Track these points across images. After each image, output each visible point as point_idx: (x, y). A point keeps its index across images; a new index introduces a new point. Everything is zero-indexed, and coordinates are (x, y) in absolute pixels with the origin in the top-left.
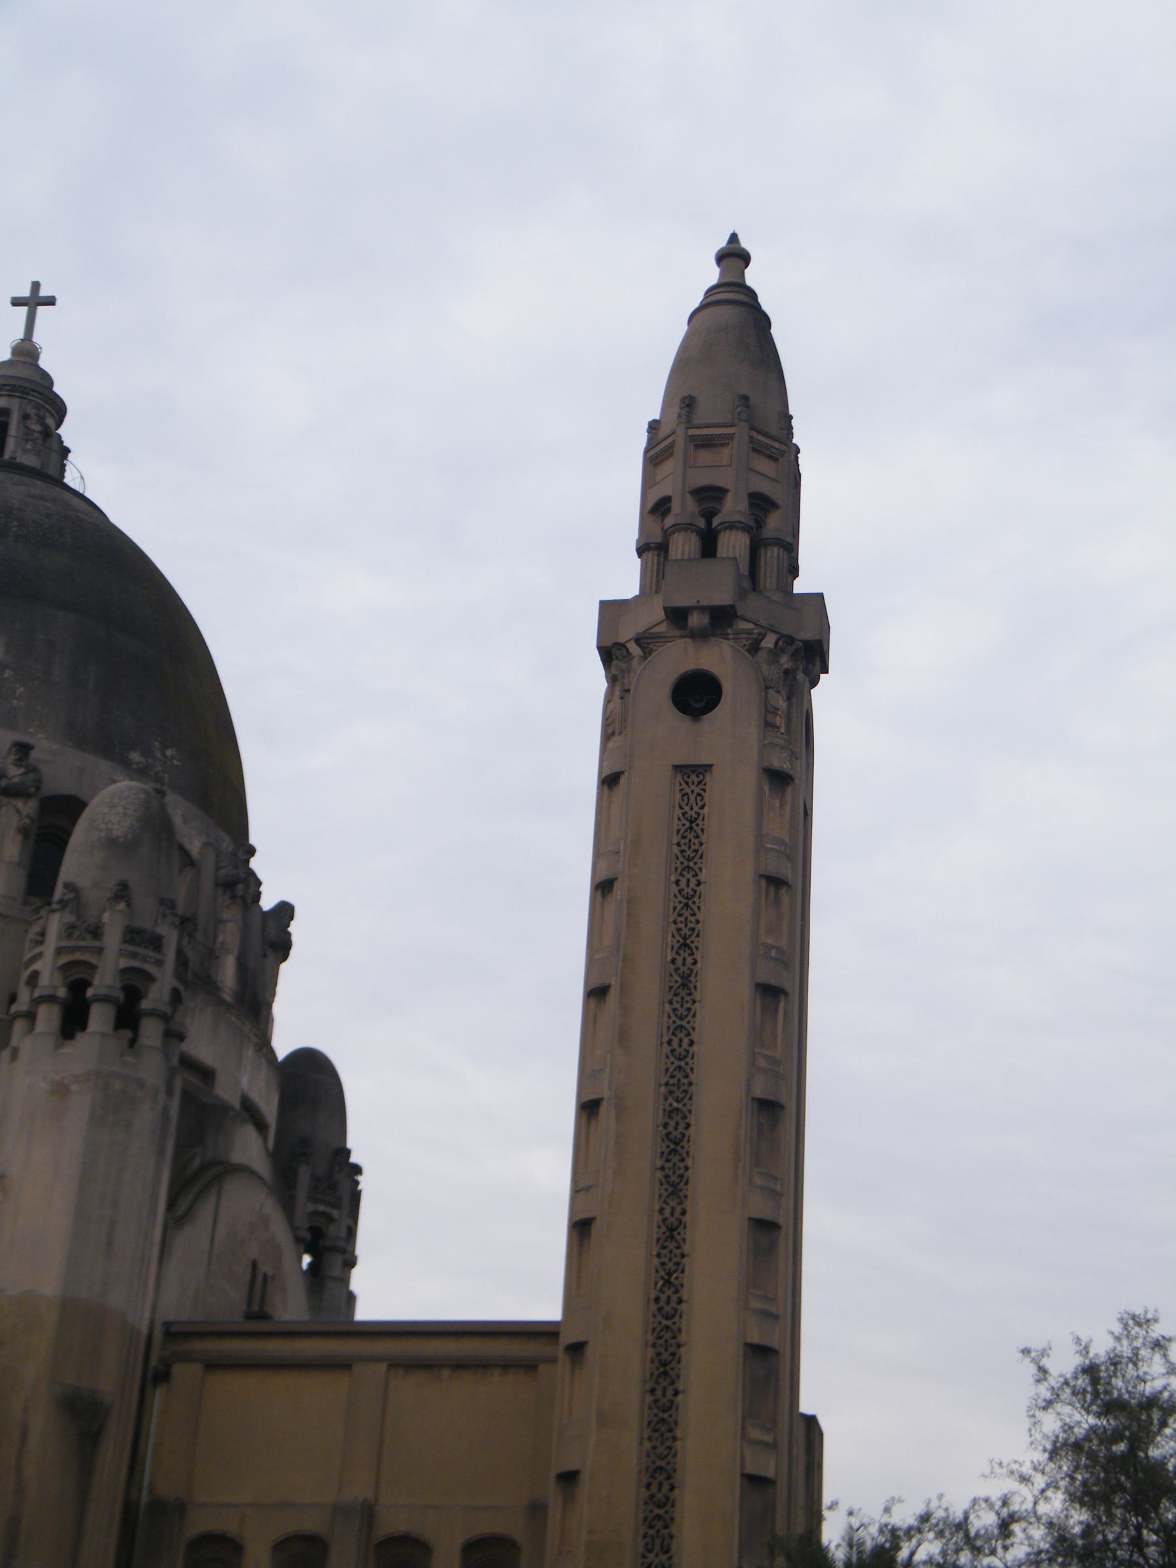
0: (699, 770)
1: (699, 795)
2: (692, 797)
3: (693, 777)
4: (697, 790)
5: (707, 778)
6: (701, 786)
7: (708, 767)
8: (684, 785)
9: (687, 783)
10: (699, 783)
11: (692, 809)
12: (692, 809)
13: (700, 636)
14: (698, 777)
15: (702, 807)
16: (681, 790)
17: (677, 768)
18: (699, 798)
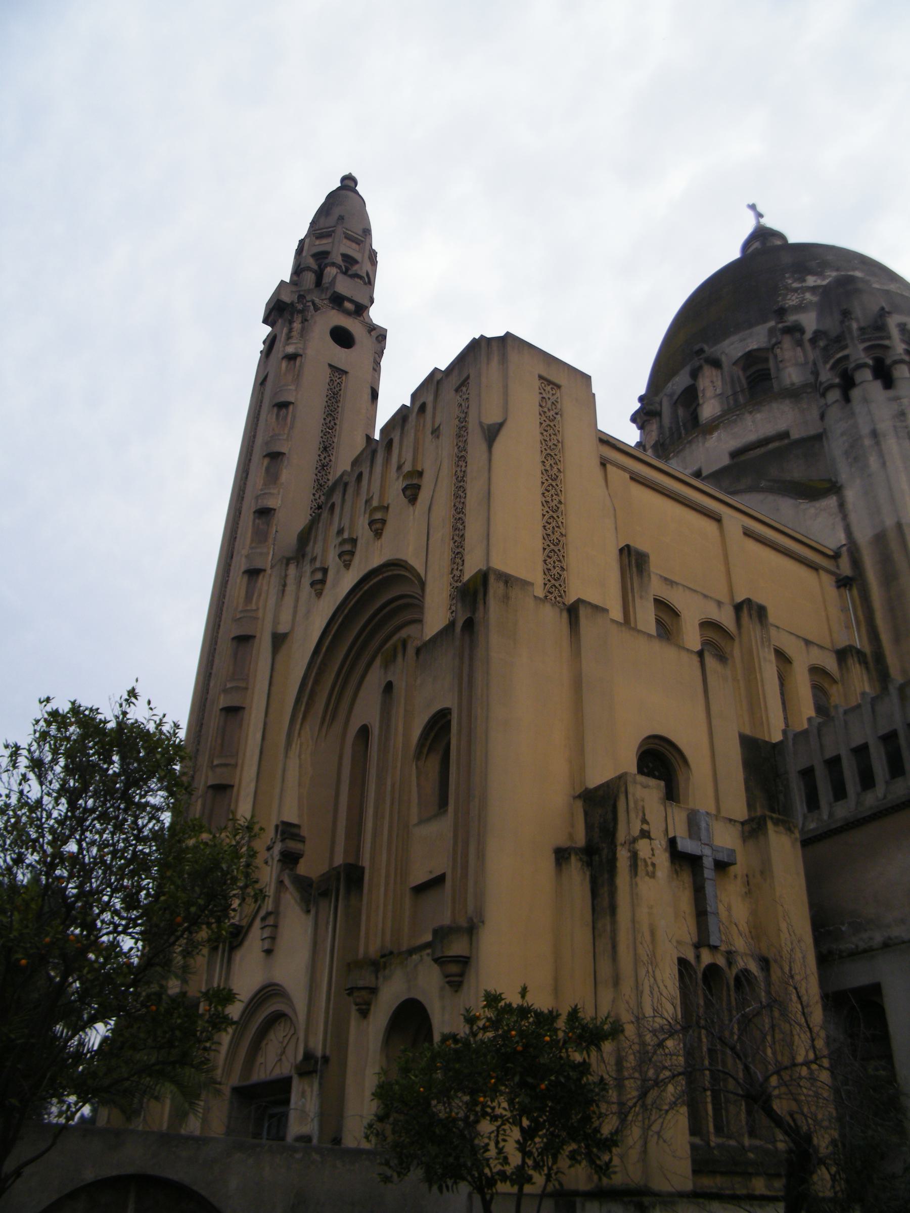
0: (341, 373)
1: (338, 383)
2: (336, 383)
3: (337, 374)
4: (338, 381)
5: (344, 377)
6: (340, 380)
7: (346, 373)
8: (332, 376)
9: (333, 375)
10: (339, 378)
11: (335, 388)
12: (335, 388)
13: (348, 313)
14: (339, 374)
15: (340, 390)
16: (330, 377)
17: (330, 365)
18: (339, 385)
